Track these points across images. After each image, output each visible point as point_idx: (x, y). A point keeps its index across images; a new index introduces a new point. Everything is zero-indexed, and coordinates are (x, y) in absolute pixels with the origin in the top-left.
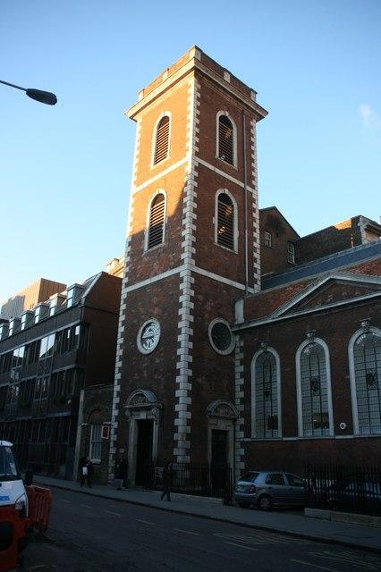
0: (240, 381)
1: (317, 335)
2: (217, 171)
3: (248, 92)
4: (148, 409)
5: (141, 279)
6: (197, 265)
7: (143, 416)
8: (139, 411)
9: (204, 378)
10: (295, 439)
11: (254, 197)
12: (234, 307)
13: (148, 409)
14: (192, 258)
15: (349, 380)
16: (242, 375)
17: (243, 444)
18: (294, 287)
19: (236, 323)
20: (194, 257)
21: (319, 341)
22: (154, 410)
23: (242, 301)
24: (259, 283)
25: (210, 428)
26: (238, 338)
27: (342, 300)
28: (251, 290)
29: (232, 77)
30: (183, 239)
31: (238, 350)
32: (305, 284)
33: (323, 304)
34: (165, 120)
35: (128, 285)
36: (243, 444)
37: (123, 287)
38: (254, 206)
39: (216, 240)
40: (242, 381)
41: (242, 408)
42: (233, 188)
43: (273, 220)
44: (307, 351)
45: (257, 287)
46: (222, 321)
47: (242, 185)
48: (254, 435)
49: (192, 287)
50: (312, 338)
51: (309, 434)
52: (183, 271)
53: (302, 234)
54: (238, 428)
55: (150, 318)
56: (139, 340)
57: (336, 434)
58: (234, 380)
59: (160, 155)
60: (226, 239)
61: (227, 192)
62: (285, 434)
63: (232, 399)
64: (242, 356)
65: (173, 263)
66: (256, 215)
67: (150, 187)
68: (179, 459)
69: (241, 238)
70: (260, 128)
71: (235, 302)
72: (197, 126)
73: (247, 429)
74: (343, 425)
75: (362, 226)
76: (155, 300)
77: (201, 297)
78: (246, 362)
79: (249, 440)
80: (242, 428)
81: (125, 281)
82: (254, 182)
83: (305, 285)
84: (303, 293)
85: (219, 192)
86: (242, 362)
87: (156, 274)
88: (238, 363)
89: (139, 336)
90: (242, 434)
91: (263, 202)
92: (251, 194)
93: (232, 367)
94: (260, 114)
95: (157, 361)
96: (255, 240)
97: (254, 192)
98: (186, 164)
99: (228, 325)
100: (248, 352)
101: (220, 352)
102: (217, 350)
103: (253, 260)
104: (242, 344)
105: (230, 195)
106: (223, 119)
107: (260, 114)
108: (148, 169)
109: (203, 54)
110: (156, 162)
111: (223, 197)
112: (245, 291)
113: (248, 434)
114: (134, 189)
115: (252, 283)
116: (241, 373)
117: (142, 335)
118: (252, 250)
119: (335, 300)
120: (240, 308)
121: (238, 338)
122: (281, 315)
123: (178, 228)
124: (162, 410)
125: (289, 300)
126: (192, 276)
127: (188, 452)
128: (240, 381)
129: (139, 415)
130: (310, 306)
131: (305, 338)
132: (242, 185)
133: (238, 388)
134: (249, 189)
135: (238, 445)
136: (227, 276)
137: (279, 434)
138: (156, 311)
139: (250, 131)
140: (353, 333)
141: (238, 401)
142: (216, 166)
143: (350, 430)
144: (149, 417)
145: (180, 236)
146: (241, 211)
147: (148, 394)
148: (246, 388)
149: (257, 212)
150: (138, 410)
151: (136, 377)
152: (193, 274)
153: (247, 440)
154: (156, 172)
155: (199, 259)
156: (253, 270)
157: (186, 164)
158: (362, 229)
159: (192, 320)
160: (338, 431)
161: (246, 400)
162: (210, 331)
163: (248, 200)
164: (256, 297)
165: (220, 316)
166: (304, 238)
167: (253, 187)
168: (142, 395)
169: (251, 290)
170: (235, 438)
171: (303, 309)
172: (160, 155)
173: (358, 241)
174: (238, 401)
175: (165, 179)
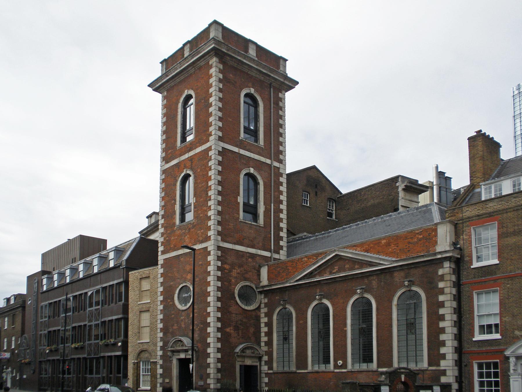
18: (308, 257)
21: (326, 302)
23: (266, 267)
29: (260, 49)
32: (317, 255)
33: (331, 273)
35: (163, 253)
37: (160, 253)
50: (320, 299)
71: (260, 267)
81: (161, 249)
92: (279, 168)
112: (271, 257)
115: (278, 249)
130: (320, 274)
131: (315, 299)
140: (351, 297)
142: (240, 148)
163: (274, 174)
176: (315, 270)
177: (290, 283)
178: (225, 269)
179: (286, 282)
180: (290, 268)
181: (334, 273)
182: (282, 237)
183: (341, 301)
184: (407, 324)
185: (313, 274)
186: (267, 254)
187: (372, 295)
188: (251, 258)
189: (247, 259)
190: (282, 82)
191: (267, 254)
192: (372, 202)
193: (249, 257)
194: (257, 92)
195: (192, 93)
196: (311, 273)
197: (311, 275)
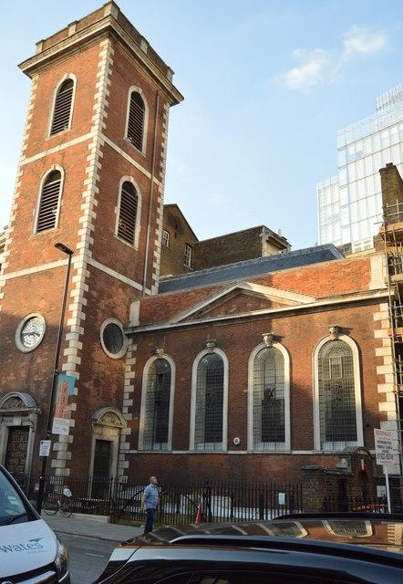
0: (129, 388)
1: (217, 346)
2: (124, 155)
3: (165, 70)
4: (24, 414)
5: (27, 265)
6: (94, 257)
7: (17, 422)
8: (12, 416)
10: (185, 452)
11: (160, 190)
12: (128, 307)
13: (24, 414)
14: (90, 249)
15: (246, 393)
16: (133, 382)
17: (128, 456)
18: (197, 293)
19: (131, 325)
20: (91, 247)
22: (32, 417)
24: (157, 285)
25: (95, 437)
26: (130, 341)
27: (246, 311)
28: (147, 291)
29: (149, 48)
30: (80, 227)
31: (130, 355)
33: (227, 313)
34: (68, 83)
36: (128, 456)
38: (159, 200)
39: (116, 232)
40: (131, 389)
41: (129, 417)
42: (140, 176)
43: (175, 218)
44: (205, 360)
45: (155, 289)
46: (115, 322)
47: (149, 175)
48: (141, 446)
49: (87, 281)
51: (201, 448)
53: (200, 240)
54: (123, 438)
55: (34, 312)
56: (18, 335)
57: (229, 448)
58: (123, 387)
59: (60, 122)
60: (127, 233)
61: (132, 180)
62: (174, 447)
63: (120, 408)
64: (133, 361)
66: (160, 211)
67: (43, 160)
68: (58, 472)
70: (174, 113)
72: (107, 98)
73: (132, 440)
74: (237, 440)
75: (265, 238)
77: (95, 294)
78: (138, 368)
79: (132, 452)
80: (128, 439)
82: (161, 174)
83: (209, 292)
84: (206, 300)
85: (124, 179)
86: (134, 368)
87: (44, 263)
88: (129, 368)
89: (19, 331)
90: (127, 446)
91: (167, 199)
93: (122, 372)
94: (175, 98)
95: (39, 360)
96: (156, 237)
97: (160, 185)
98: (90, 141)
99: (121, 326)
100: (141, 358)
103: (152, 259)
104: (135, 348)
105: (135, 185)
106: (135, 95)
107: (175, 98)
108: (41, 139)
109: (120, 14)
110: (54, 131)
111: (128, 185)
113: (134, 446)
115: (150, 284)
116: (131, 379)
117: (23, 329)
118: (153, 248)
119: (239, 311)
120: (135, 309)
121: (130, 341)
123: (76, 213)
124: (40, 416)
125: (190, 305)
126: (88, 269)
127: (68, 464)
128: (129, 388)
129: (12, 421)
130: (212, 314)
132: (149, 175)
133: (126, 396)
134: (155, 180)
135: (122, 457)
136: (125, 274)
137: (168, 447)
138: (42, 304)
139: (162, 116)
141: (125, 410)
143: (243, 445)
144: (25, 424)
145: (77, 222)
146: (147, 203)
147: (25, 398)
148: (136, 396)
149: (162, 207)
150: (12, 415)
152: (89, 267)
153: (132, 452)
154: (51, 146)
155: (96, 250)
156: (152, 270)
157: (90, 141)
158: (264, 241)
160: (231, 446)
161: (135, 410)
162: (102, 331)
163: (153, 195)
164: (153, 301)
165: (114, 316)
166: (203, 242)
167: (160, 179)
168: (18, 398)
169: (147, 291)
170: (119, 449)
171: (204, 317)
172: (60, 122)
173: (258, 253)
174: (125, 410)
175: (63, 153)
176: (206, 308)
177: (172, 324)
179: (167, 319)
183: (241, 352)
186: (139, 287)
191: (139, 287)
192: (232, 252)
196: (200, 312)
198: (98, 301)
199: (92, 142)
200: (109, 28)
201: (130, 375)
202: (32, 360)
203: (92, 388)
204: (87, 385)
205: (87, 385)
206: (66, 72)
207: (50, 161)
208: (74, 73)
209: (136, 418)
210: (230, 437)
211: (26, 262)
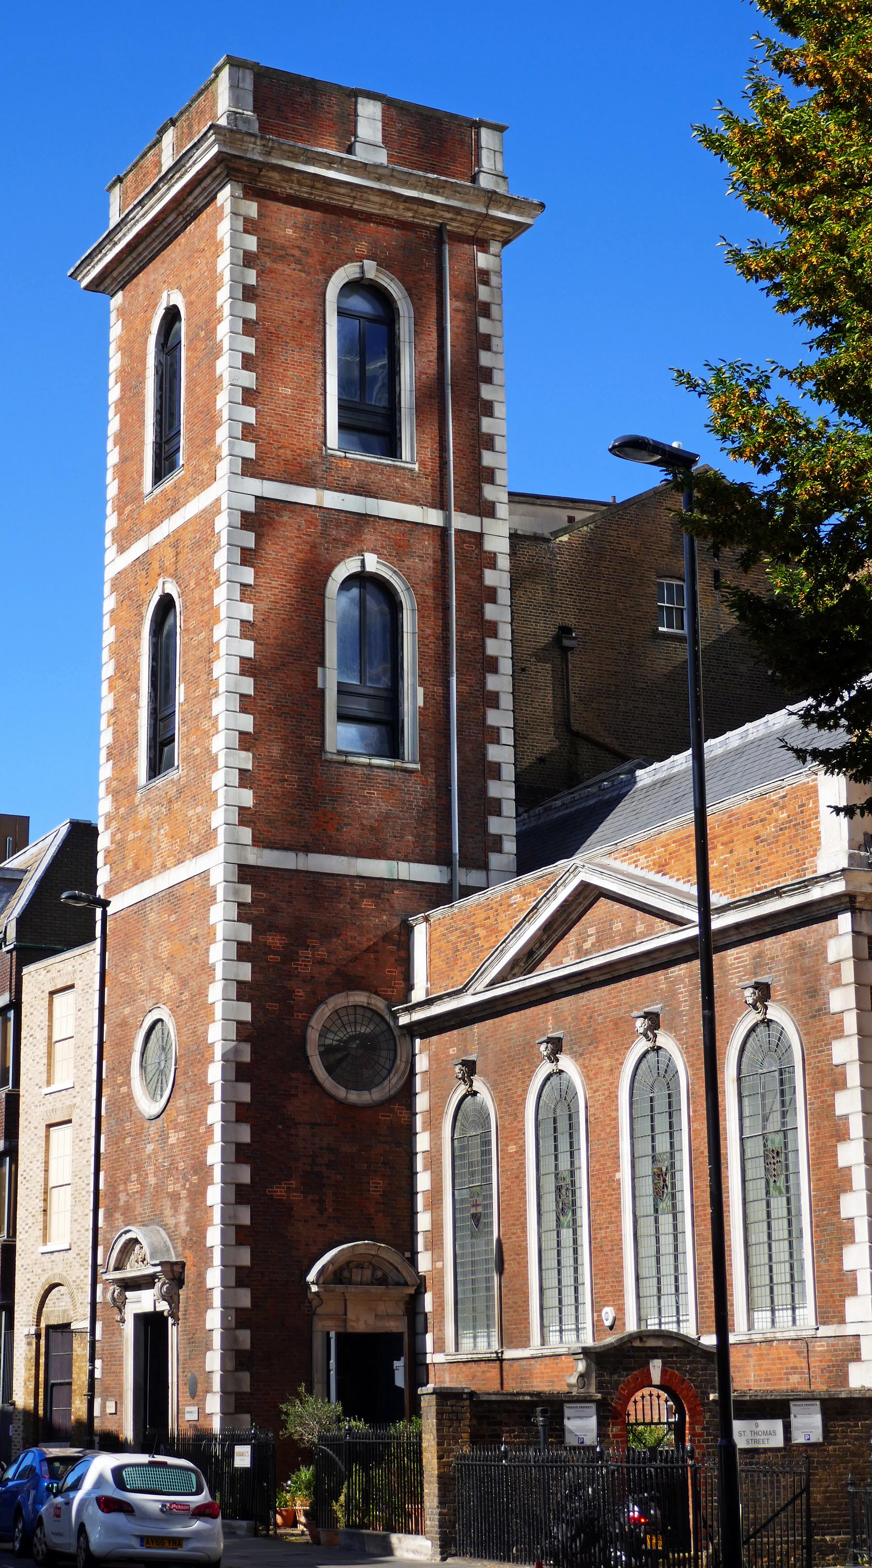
9: (294, 1183)
15: (618, 1182)
20: (245, 817)
24: (510, 846)
52: (215, 864)
65: (195, 839)
67: (143, 561)
69: (438, 705)
76: (165, 948)
85: (348, 567)
87: (164, 867)
95: (172, 1140)
101: (353, 1097)
102: (341, 1092)
108: (140, 496)
110: (158, 476)
112: (450, 885)
114: (115, 562)
122: (493, 984)
145: (208, 751)
151: (133, 1187)
152: (245, 873)
159: (248, 1017)
175: (175, 541)
178: (271, 950)
180: (481, 932)
181: (588, 952)
182: (498, 801)
184: (766, 1157)
185: (536, 956)
187: (679, 1039)
188: (371, 896)
189: (354, 904)
190: (480, 214)
193: (363, 894)
194: (387, 267)
195: (177, 299)
197: (528, 959)
198: (289, 956)
199: (219, 512)
200: (219, 159)
201: (423, 1142)
202: (163, 1136)
203: (296, 1197)
204: (279, 1191)
205: (279, 1191)
206: (165, 288)
207: (156, 565)
208: (179, 288)
209: (439, 1265)
210: (596, 1308)
211: (136, 866)
